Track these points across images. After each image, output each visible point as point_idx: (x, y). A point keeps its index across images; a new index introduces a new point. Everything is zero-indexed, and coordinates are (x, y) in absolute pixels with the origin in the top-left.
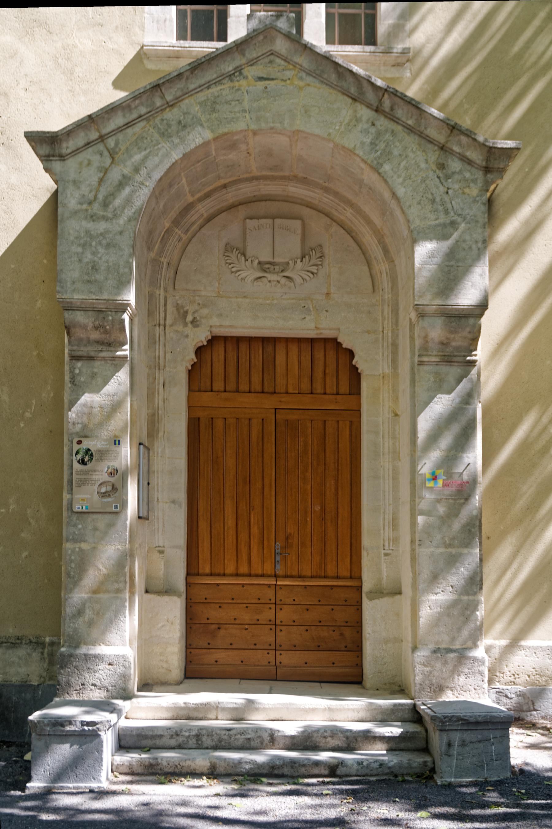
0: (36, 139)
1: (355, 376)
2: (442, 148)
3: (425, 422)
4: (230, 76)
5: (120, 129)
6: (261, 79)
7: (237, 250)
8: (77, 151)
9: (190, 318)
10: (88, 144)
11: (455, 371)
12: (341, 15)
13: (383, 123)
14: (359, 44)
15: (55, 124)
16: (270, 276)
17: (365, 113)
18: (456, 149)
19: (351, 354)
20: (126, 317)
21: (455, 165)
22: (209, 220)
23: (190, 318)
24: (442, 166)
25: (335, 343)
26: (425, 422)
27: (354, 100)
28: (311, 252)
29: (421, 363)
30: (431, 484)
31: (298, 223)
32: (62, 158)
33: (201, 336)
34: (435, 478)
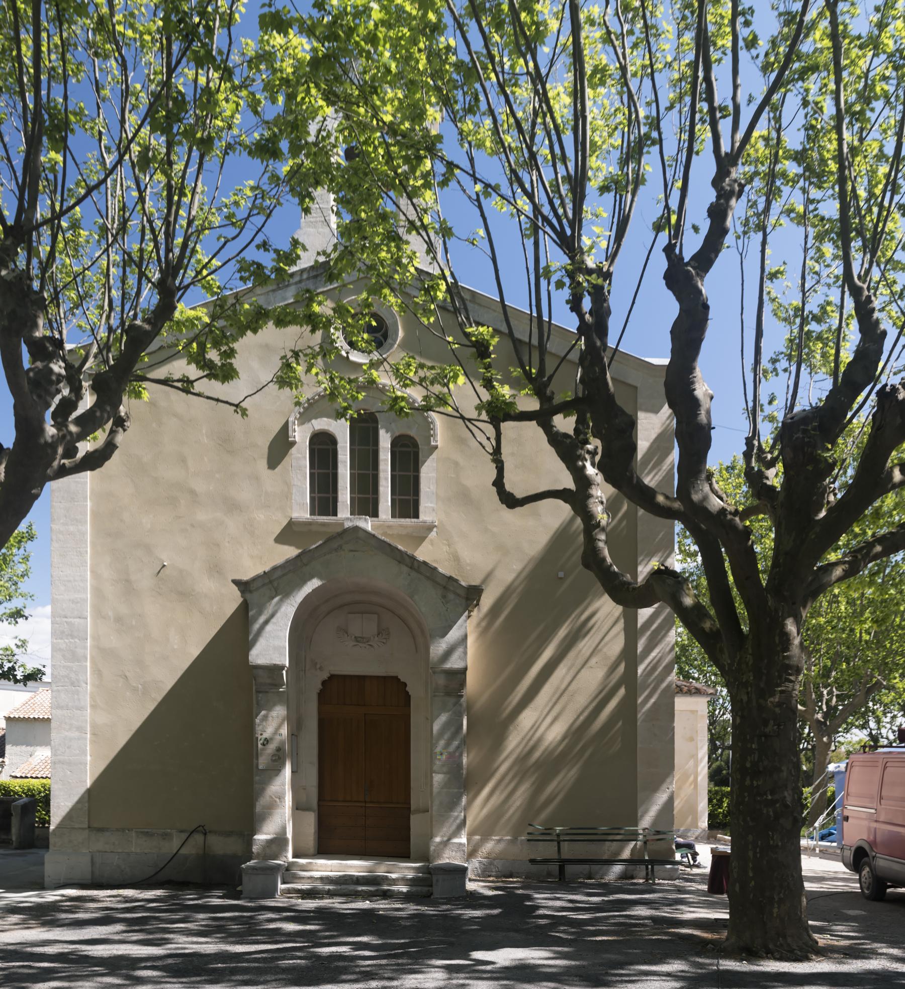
0: (236, 582)
1: (408, 697)
2: (444, 587)
3: (436, 727)
4: (336, 550)
5: (280, 577)
6: (352, 551)
7: (343, 630)
8: (258, 589)
9: (318, 666)
10: (264, 585)
11: (452, 700)
12: (400, 500)
13: (414, 574)
14: (410, 517)
15: (246, 577)
16: (360, 644)
17: (405, 569)
18: (452, 588)
19: (405, 685)
20: (284, 672)
21: (451, 596)
22: (329, 613)
23: (318, 666)
24: (444, 597)
25: (396, 679)
26: (436, 727)
27: (400, 562)
28: (383, 632)
29: (435, 696)
30: (439, 757)
31: (376, 616)
32: (251, 592)
33: (325, 676)
34: (441, 754)
